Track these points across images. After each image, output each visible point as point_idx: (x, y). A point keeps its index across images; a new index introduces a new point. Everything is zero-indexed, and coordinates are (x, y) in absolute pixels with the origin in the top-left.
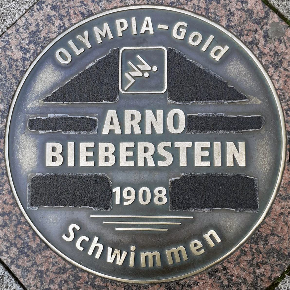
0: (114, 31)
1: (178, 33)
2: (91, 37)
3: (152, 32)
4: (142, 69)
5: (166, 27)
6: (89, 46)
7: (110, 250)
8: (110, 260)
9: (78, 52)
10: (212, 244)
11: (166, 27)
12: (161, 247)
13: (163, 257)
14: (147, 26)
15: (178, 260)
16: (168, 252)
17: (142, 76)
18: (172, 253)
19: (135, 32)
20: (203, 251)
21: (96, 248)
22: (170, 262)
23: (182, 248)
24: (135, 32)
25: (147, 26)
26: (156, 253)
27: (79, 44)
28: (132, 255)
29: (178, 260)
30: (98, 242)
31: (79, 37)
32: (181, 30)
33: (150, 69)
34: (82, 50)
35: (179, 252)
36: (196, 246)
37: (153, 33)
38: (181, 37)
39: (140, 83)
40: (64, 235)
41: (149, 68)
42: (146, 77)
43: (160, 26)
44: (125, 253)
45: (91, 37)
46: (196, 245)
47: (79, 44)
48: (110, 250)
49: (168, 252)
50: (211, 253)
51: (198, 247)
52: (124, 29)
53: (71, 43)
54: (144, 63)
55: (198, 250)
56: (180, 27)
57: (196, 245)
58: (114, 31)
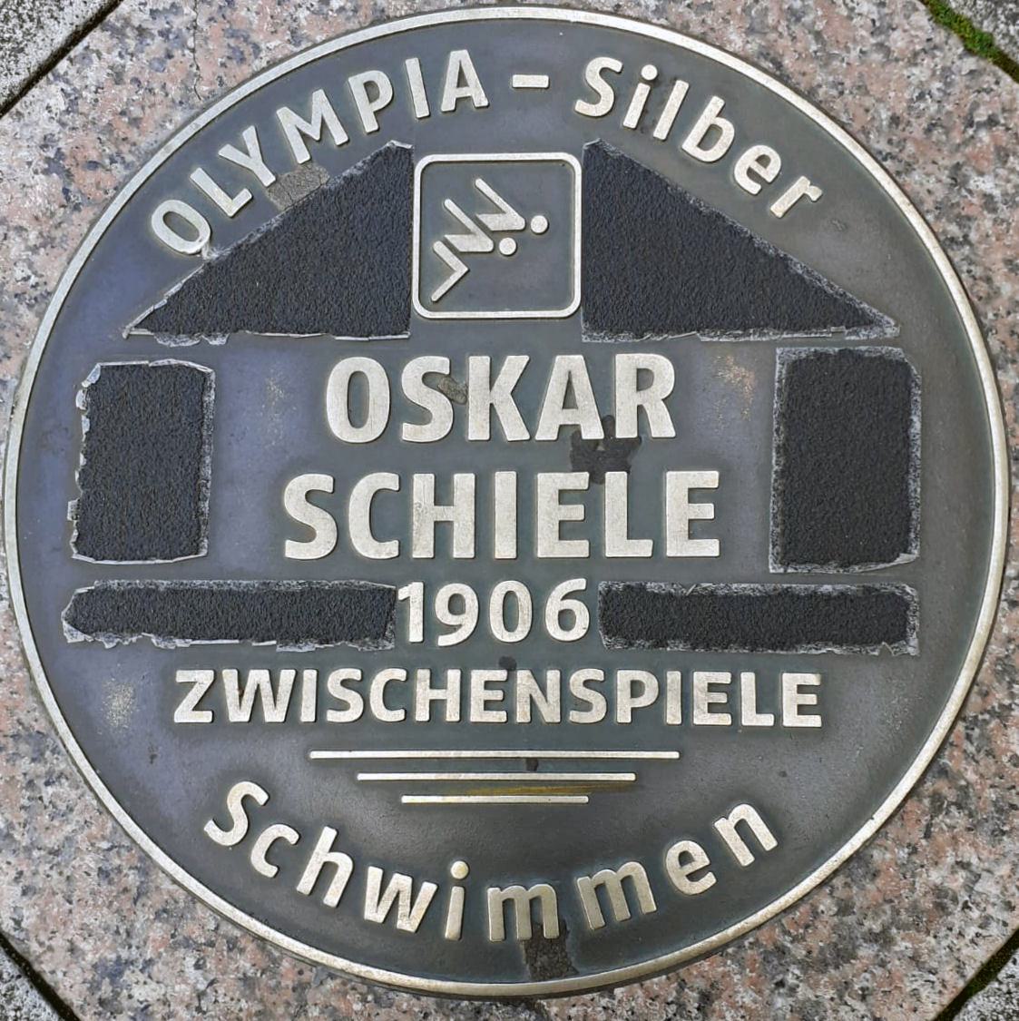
0: (349, 119)
2: (274, 151)
3: (481, 100)
4: (492, 227)
7: (374, 875)
8: (374, 912)
10: (745, 857)
12: (560, 869)
13: (567, 899)
14: (462, 81)
15: (621, 912)
16: (584, 884)
17: (494, 250)
18: (600, 889)
20: (709, 880)
21: (328, 870)
22: (593, 918)
23: (634, 869)
25: (462, 81)
26: (543, 890)
28: (457, 894)
29: (621, 912)
30: (334, 848)
33: (522, 227)
35: (627, 882)
36: (685, 864)
37: (485, 103)
39: (486, 278)
40: (211, 823)
41: (519, 223)
42: (503, 252)
44: (428, 889)
45: (274, 151)
46: (685, 858)
48: (374, 875)
49: (584, 884)
50: (738, 889)
51: (689, 868)
52: (379, 104)
54: (501, 206)
55: (693, 877)
57: (685, 858)
58: (349, 119)
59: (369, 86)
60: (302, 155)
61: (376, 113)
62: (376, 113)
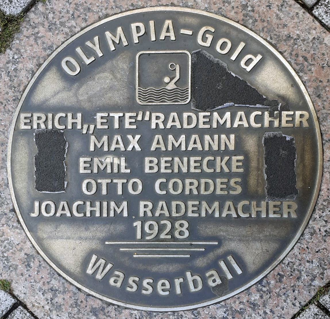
1: (204, 39)
3: (173, 38)
5: (190, 32)
6: (100, 55)
9: (88, 61)
11: (190, 32)
19: (153, 38)
24: (153, 38)
27: (89, 52)
31: (89, 44)
32: (207, 36)
34: (93, 59)
38: (208, 44)
43: (183, 31)
47: (89, 52)
53: (79, 50)
55: (212, 275)
56: (207, 32)
59: (138, 28)
60: (112, 48)
61: (138, 37)
62: (138, 37)
